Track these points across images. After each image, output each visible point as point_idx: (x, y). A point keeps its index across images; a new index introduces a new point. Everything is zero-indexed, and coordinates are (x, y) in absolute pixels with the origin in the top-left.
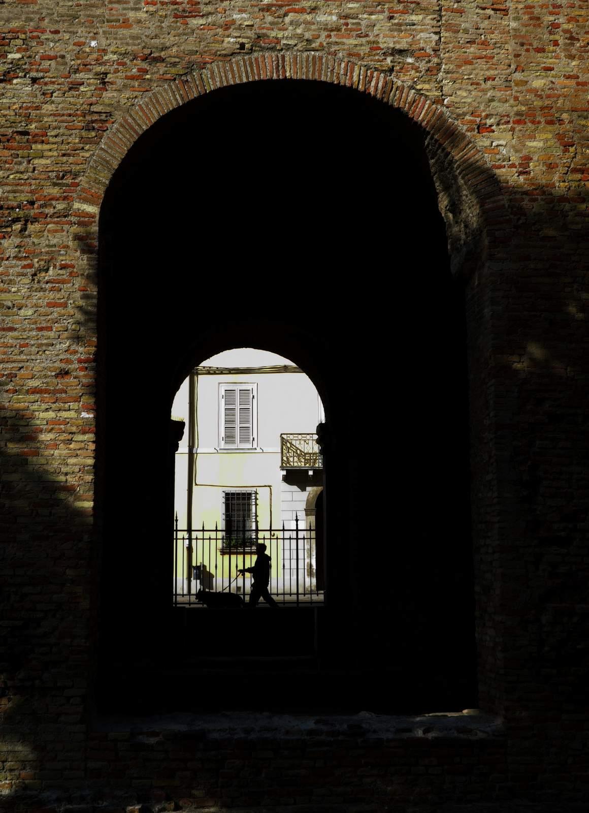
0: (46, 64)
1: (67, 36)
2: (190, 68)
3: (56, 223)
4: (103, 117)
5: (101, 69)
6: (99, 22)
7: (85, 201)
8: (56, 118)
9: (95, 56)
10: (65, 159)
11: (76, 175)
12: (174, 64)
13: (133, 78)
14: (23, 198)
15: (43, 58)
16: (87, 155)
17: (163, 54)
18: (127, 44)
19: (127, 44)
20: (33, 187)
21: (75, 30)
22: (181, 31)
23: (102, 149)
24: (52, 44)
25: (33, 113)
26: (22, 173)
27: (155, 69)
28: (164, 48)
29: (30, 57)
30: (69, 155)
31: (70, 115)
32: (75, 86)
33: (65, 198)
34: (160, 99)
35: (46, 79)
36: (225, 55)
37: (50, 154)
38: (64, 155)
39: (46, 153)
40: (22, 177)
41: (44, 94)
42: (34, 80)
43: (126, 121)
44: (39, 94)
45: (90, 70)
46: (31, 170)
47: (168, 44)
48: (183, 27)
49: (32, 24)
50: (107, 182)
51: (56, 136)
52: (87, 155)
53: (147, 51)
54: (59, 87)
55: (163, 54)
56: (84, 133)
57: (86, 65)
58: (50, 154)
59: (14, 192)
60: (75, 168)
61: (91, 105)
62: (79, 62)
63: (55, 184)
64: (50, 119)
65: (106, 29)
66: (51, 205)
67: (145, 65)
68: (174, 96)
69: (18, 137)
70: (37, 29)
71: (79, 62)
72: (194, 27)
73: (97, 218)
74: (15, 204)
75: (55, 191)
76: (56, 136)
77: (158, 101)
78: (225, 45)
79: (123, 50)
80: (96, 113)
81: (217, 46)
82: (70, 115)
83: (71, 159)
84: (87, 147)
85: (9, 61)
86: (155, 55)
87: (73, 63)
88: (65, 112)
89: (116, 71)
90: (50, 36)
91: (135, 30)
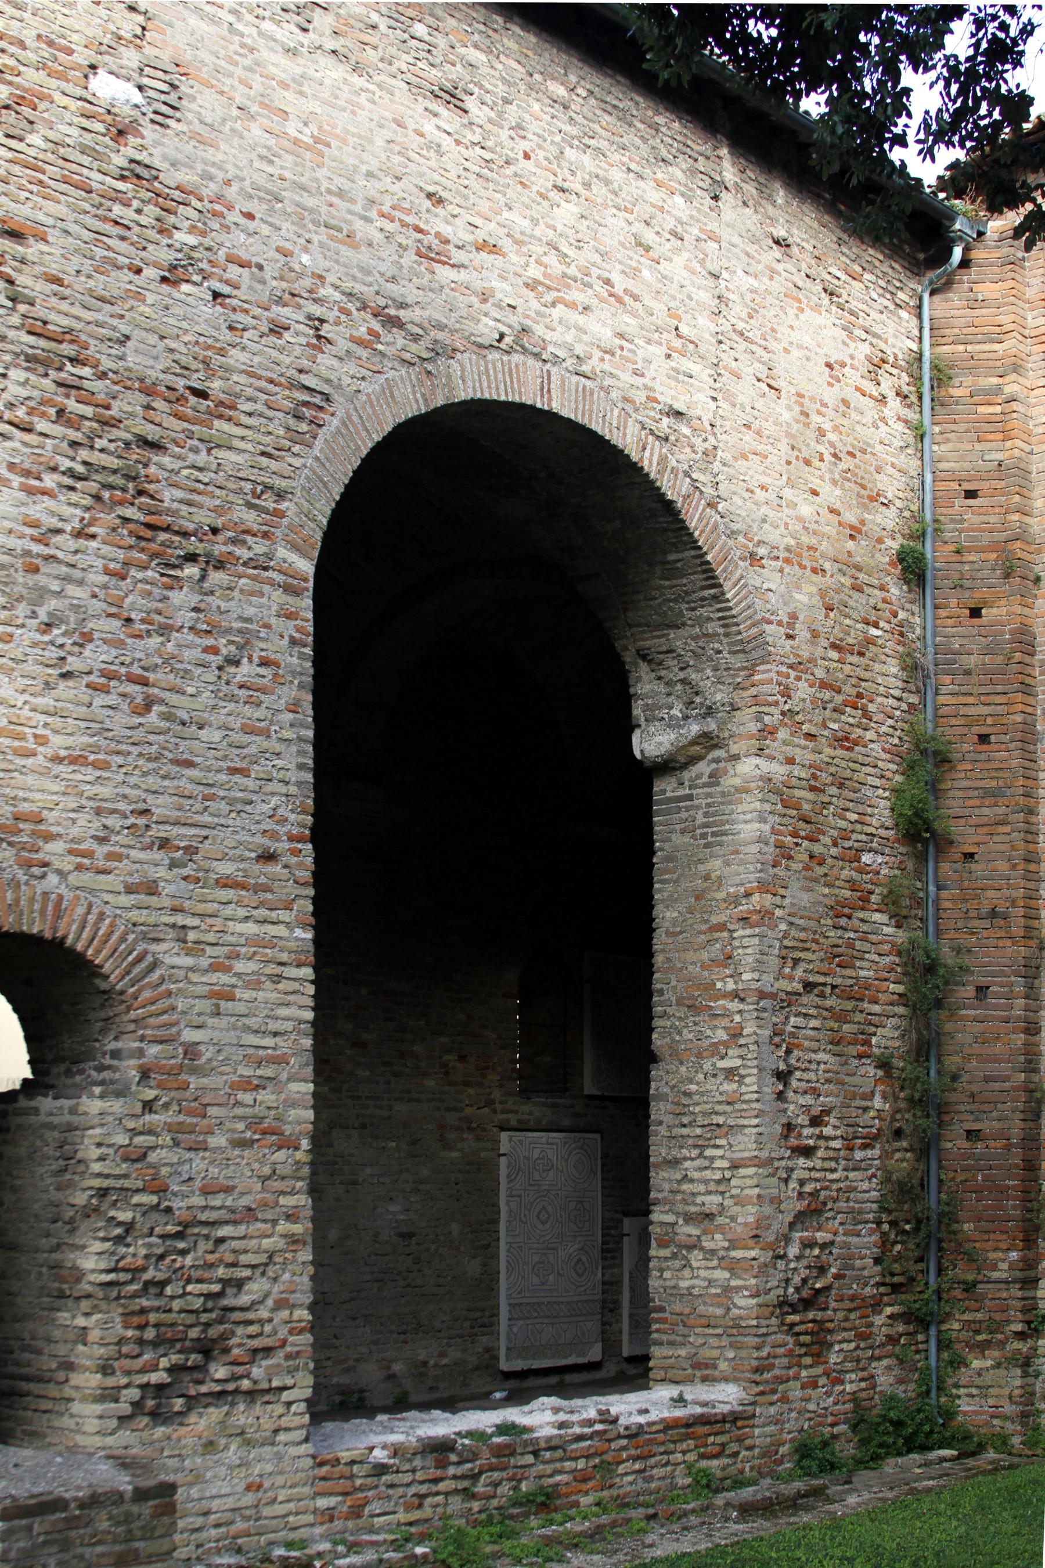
0: (234, 272)
1: (266, 230)
2: (438, 351)
3: (253, 578)
4: (317, 400)
5: (318, 311)
6: (313, 221)
7: (295, 547)
8: (252, 380)
9: (308, 282)
10: (264, 461)
11: (281, 495)
12: (416, 338)
13: (359, 342)
14: (204, 518)
15: (230, 259)
16: (297, 462)
17: (402, 313)
18: (354, 278)
19: (354, 278)
20: (218, 502)
21: (278, 223)
22: (424, 282)
23: (317, 459)
24: (243, 237)
25: (217, 360)
26: (200, 469)
27: (389, 338)
28: (403, 306)
29: (209, 249)
30: (269, 456)
31: (271, 381)
32: (277, 329)
33: (266, 535)
34: (396, 393)
35: (235, 302)
36: (481, 346)
37: (242, 445)
38: (263, 454)
39: (237, 443)
40: (201, 476)
41: (231, 328)
42: (216, 295)
43: (349, 417)
44: (224, 326)
45: (299, 307)
46: (214, 467)
47: (409, 300)
48: (428, 276)
49: (212, 185)
50: (325, 522)
51: (250, 414)
52: (297, 462)
53: (382, 302)
54: (254, 322)
55: (402, 313)
56: (292, 422)
57: (293, 295)
58: (242, 445)
59: (189, 503)
60: (278, 482)
61: (301, 371)
62: (284, 285)
63: (250, 506)
64: (243, 379)
65: (323, 238)
66: (244, 542)
67: (376, 326)
68: (414, 393)
69: (193, 400)
70: (218, 199)
71: (284, 285)
72: (445, 281)
73: (311, 584)
74: (191, 527)
75: (251, 518)
76: (250, 414)
77: (392, 396)
78: (481, 326)
79: (347, 285)
80: (308, 388)
81: (470, 327)
82: (271, 381)
83: (274, 465)
84: (296, 449)
85: (178, 246)
86: (392, 312)
87: (274, 283)
88: (264, 373)
89: (337, 323)
90: (242, 221)
91: (364, 256)
